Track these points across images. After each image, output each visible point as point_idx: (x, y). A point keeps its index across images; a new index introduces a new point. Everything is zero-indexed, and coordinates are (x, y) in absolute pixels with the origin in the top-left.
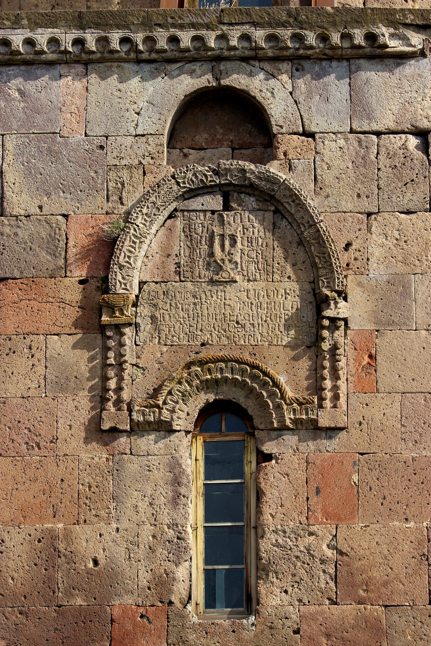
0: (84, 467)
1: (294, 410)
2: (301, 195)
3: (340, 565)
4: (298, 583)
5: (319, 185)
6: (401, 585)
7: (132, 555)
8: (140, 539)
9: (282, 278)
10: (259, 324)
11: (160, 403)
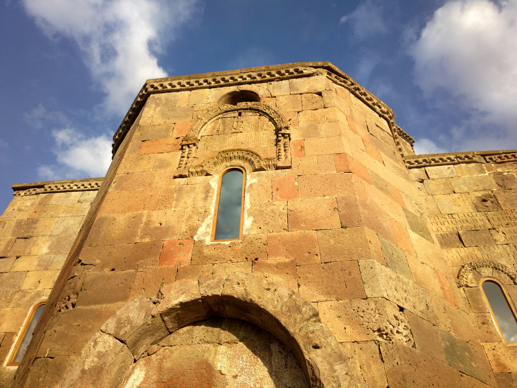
1: (266, 162)
6: (324, 221)
7: (180, 220)
11: (203, 165)
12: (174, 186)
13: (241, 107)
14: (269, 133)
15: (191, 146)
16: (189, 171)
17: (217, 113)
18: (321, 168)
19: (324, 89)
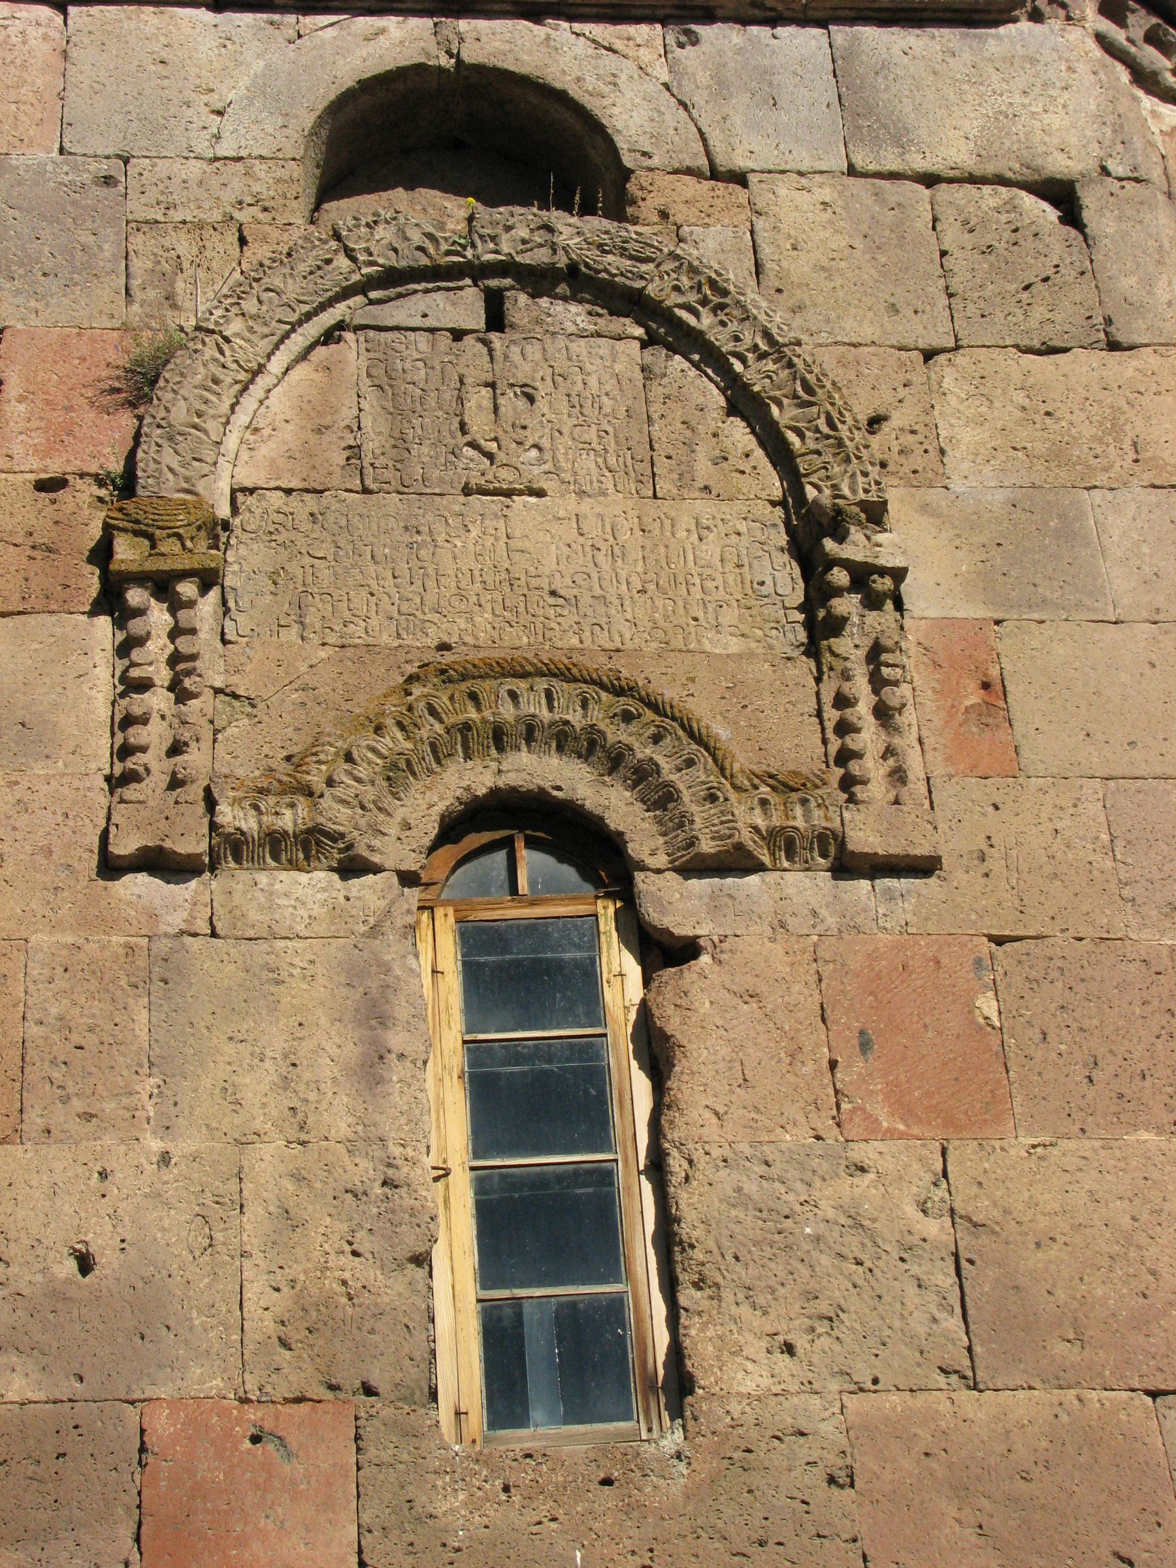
0: (47, 972)
1: (764, 803)
2: (727, 280)
3: (971, 1262)
4: (830, 1319)
5: (771, 280)
7: (219, 1236)
8: (248, 1187)
9: (685, 491)
10: (620, 597)
11: (316, 780)
12: (117, 939)
13: (506, 247)
14: (742, 527)
15: (187, 589)
16: (213, 826)
17: (331, 282)
18: (1138, 891)
19: (1092, 165)
